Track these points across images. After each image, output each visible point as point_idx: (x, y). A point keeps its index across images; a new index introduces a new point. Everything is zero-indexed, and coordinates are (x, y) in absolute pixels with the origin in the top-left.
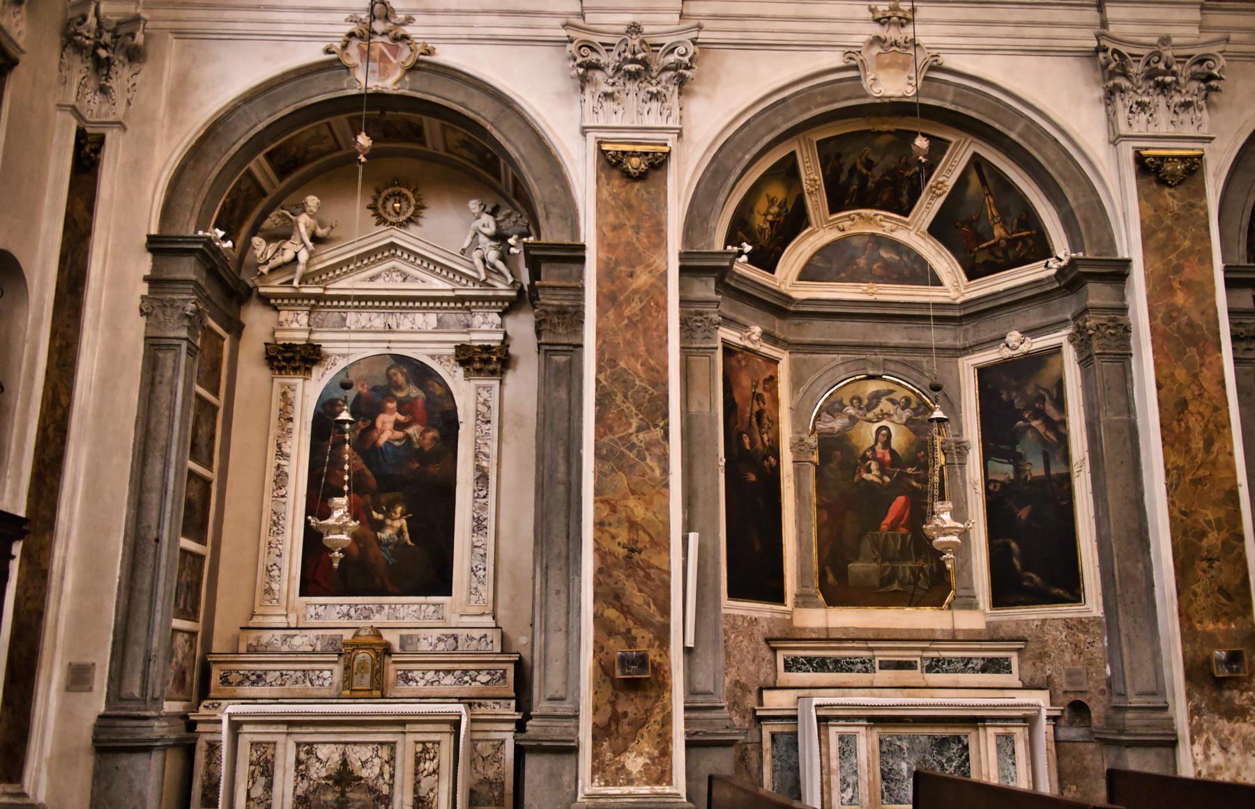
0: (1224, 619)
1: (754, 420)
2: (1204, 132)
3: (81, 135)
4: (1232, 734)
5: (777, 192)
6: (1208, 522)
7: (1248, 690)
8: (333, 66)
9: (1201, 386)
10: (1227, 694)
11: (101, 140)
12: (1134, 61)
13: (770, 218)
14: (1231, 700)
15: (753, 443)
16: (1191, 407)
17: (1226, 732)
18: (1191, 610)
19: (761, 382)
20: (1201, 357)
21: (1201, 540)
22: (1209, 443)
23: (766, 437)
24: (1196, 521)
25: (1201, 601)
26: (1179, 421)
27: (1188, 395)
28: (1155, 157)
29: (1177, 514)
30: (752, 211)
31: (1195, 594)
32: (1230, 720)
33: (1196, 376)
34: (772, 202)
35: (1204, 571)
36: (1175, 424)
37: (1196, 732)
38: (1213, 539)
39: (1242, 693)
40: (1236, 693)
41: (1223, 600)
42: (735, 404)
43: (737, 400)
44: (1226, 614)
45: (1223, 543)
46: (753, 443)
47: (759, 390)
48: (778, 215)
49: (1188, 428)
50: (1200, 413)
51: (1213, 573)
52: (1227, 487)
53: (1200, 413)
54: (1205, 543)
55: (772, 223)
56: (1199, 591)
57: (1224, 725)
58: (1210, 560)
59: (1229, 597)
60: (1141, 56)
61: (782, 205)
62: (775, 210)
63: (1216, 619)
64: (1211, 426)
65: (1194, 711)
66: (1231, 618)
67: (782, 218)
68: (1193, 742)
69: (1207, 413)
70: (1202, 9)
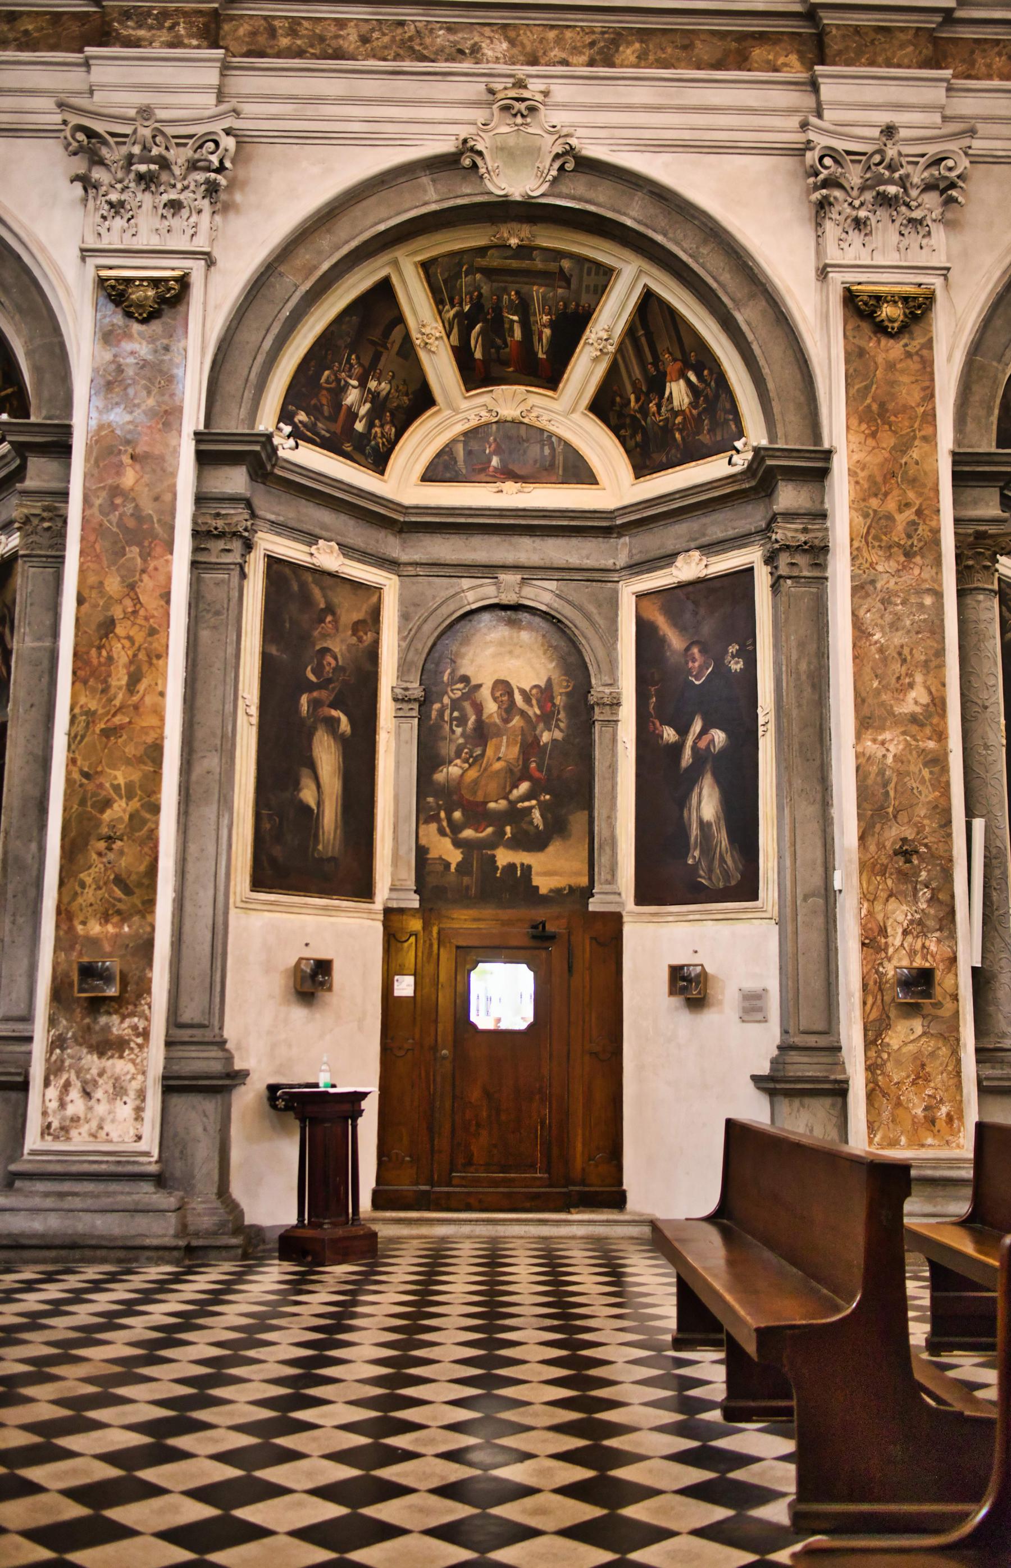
0: (115, 919)
2: (201, 243)
4: (101, 1074)
6: (116, 788)
7: (132, 1014)
9: (137, 601)
10: (103, 1020)
12: (852, 161)
14: (107, 1028)
16: (119, 630)
17: (94, 1071)
18: (74, 907)
20: (145, 560)
21: (102, 811)
22: (134, 679)
24: (101, 786)
25: (89, 895)
26: (100, 648)
27: (117, 612)
28: (117, 279)
29: (76, 776)
31: (83, 885)
32: (101, 1054)
33: (132, 587)
35: (100, 854)
36: (93, 652)
37: (53, 1071)
38: (120, 810)
39: (123, 1018)
40: (115, 1019)
41: (118, 893)
44: (119, 912)
45: (132, 817)
49: (110, 659)
50: (129, 638)
51: (111, 856)
52: (149, 740)
53: (129, 638)
54: (107, 816)
56: (89, 880)
57: (92, 1062)
58: (109, 839)
59: (128, 891)
60: (864, 154)
63: (106, 918)
64: (142, 656)
65: (58, 1043)
66: (124, 917)
68: (47, 1083)
69: (139, 637)
70: (949, 90)
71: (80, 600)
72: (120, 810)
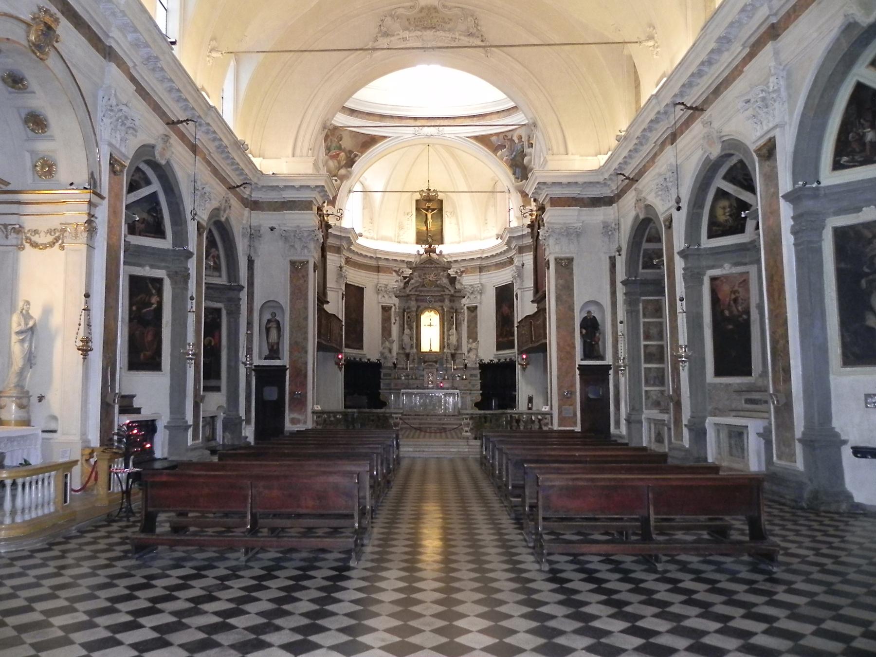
1: (732, 302)
3: (610, 258)
5: (724, 203)
8: (637, 216)
11: (615, 257)
13: (727, 214)
15: (731, 312)
16: (775, 279)
19: (737, 285)
23: (740, 308)
30: (716, 217)
34: (724, 208)
42: (719, 300)
43: (720, 296)
46: (731, 312)
47: (736, 288)
48: (732, 210)
55: (730, 215)
61: (730, 206)
62: (728, 210)
67: (735, 211)
71: (766, 270)
72: (782, 342)
